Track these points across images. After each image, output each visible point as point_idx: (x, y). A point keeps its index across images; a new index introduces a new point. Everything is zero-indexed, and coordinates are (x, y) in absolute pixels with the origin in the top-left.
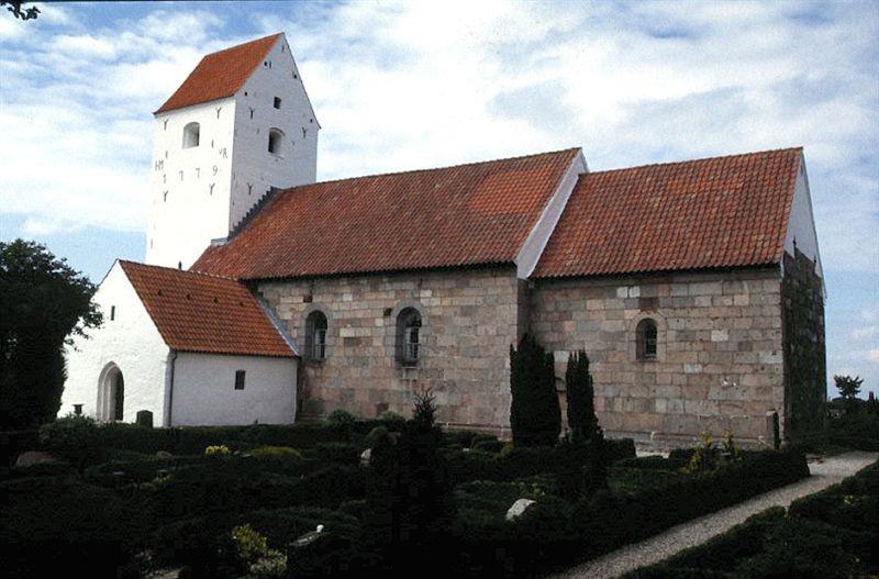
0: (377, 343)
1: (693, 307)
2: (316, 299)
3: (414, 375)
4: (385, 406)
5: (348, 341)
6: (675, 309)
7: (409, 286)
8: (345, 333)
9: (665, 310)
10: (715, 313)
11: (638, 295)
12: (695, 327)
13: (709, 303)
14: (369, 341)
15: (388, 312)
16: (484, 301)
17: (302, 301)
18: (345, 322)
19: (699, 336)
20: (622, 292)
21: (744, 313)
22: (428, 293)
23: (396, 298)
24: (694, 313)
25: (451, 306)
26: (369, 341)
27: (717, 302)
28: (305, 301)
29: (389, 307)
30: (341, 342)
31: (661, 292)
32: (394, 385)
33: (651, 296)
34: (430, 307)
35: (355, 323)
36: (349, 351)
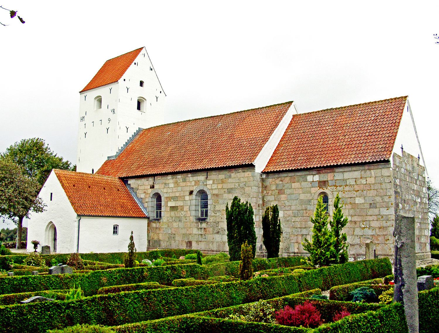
0: (186, 208)
1: (346, 185)
2: (156, 186)
3: (204, 225)
4: (190, 243)
5: (173, 208)
6: (337, 186)
7: (201, 177)
8: (171, 204)
9: (332, 187)
10: (357, 188)
11: (318, 180)
12: (347, 196)
13: (354, 183)
14: (182, 208)
15: (191, 193)
16: (239, 185)
17: (149, 187)
18: (169, 199)
20: (310, 178)
21: (372, 187)
22: (211, 182)
23: (195, 185)
24: (347, 188)
25: (222, 188)
26: (182, 208)
27: (358, 182)
28: (151, 188)
29: (192, 190)
30: (169, 208)
31: (328, 176)
32: (195, 231)
33: (325, 180)
34: (212, 189)
35: (175, 198)
36: (173, 213)
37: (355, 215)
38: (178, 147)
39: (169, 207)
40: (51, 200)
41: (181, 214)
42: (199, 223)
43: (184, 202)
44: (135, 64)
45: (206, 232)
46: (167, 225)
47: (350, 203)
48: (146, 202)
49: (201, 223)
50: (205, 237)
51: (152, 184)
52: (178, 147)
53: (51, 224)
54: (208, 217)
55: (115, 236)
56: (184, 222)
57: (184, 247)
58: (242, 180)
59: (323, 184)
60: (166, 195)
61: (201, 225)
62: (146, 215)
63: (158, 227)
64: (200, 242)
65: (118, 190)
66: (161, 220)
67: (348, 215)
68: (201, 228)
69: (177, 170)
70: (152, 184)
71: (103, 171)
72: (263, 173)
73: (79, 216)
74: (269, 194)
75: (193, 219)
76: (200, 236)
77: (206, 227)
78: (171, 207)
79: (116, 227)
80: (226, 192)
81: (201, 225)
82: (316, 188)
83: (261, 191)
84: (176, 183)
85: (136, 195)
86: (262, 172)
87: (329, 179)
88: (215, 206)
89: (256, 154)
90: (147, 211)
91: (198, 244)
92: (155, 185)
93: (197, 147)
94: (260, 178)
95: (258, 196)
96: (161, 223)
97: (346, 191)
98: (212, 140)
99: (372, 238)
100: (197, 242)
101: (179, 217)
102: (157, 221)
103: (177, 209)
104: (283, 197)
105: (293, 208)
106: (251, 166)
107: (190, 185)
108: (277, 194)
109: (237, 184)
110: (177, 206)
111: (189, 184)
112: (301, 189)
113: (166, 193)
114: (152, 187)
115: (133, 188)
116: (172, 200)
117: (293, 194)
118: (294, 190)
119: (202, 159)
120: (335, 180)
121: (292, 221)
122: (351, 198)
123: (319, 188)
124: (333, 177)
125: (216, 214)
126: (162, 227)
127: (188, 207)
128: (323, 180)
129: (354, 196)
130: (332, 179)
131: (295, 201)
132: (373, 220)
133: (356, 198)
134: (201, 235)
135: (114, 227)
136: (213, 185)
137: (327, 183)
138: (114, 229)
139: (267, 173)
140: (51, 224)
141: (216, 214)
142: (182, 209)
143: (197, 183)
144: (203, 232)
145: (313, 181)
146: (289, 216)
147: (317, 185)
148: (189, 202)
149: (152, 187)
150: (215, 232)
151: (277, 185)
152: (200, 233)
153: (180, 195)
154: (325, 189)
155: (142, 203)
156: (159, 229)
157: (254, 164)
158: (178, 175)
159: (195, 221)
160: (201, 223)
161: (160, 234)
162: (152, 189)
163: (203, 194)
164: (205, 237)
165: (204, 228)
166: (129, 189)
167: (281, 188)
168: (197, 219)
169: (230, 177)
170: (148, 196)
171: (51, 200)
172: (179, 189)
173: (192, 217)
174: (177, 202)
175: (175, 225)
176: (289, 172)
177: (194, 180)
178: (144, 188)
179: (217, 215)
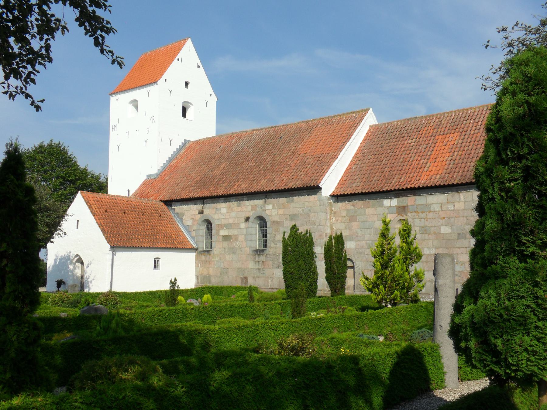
0: (242, 238)
1: (430, 211)
2: (206, 212)
3: (262, 258)
4: (246, 279)
5: (226, 238)
6: (419, 213)
7: (259, 202)
8: (223, 233)
9: (413, 214)
11: (396, 204)
12: (430, 225)
13: (439, 209)
14: (236, 238)
15: (247, 219)
16: (303, 210)
17: (198, 212)
18: (221, 226)
19: (433, 229)
20: (387, 202)
22: (270, 207)
23: (252, 210)
24: (431, 215)
25: (284, 215)
26: (236, 238)
27: (444, 208)
28: (199, 213)
29: (248, 216)
30: (221, 238)
31: (409, 200)
32: (251, 265)
33: (405, 204)
34: (271, 215)
35: (228, 226)
36: (225, 244)
37: (441, 247)
38: (232, 164)
39: (221, 237)
40: (77, 228)
41: (235, 244)
42: (257, 256)
43: (239, 230)
44: (178, 60)
45: (265, 266)
46: (219, 258)
47: (435, 233)
48: (194, 230)
49: (259, 255)
50: (263, 272)
51: (201, 209)
52: (232, 164)
53: (78, 257)
54: (268, 249)
55: (156, 271)
56: (238, 254)
57: (239, 284)
58: (306, 204)
59: (402, 209)
60: (217, 223)
61: (259, 257)
62: (194, 246)
63: (208, 260)
64: (257, 279)
65: (160, 216)
66: (212, 252)
67: (432, 247)
68: (259, 262)
69: (231, 192)
70: (201, 209)
71: (141, 193)
72: (332, 196)
73: (112, 247)
74: (339, 221)
75: (248, 250)
76: (257, 271)
77: (264, 260)
78: (223, 236)
79: (158, 261)
80: (288, 219)
81: (259, 257)
82: (394, 214)
83: (329, 217)
84: (229, 208)
85: (182, 221)
86: (330, 195)
87: (409, 204)
88: (275, 235)
89: (322, 174)
90: (194, 241)
91: (256, 281)
92: (204, 210)
93: (254, 164)
94: (328, 202)
95: (325, 223)
96: (212, 255)
97: (430, 219)
98: (273, 156)
99: (461, 274)
100: (254, 277)
101: (233, 248)
102: (206, 253)
103: (230, 239)
104: (355, 225)
105: (367, 237)
106: (315, 189)
107: (246, 210)
108: (348, 221)
109: (301, 210)
110: (231, 236)
111: (244, 209)
112: (376, 216)
113: (218, 219)
114: (201, 212)
115: (178, 213)
116: (225, 228)
117: (367, 221)
118: (368, 216)
119: (261, 179)
120: (417, 205)
121: (366, 253)
122: (435, 226)
123: (397, 215)
124: (415, 201)
125: (276, 244)
126: (213, 260)
127: (243, 236)
128: (402, 205)
129: (440, 224)
130: (413, 204)
131: (369, 230)
132: (462, 253)
133: (442, 227)
134: (259, 269)
135: (155, 261)
136: (273, 210)
137: (406, 208)
138: (155, 262)
139: (337, 197)
140: (78, 257)
141: (276, 244)
142: (236, 239)
143: (254, 208)
144: (261, 266)
145: (391, 206)
146: (362, 247)
147: (395, 210)
148: (245, 230)
149: (201, 212)
150: (275, 266)
151: (348, 210)
152: (257, 267)
153: (234, 221)
154: (405, 216)
155: (189, 232)
156: (209, 262)
157: (321, 187)
158: (232, 198)
159: (251, 253)
160: (259, 255)
161: (211, 269)
162: (201, 215)
163: (262, 221)
164: (263, 272)
165: (262, 262)
166: (173, 215)
167: (353, 215)
168: (254, 251)
169: (293, 201)
170: (196, 222)
171: (77, 228)
172: (233, 214)
173: (248, 248)
174: (231, 230)
175: (228, 257)
176: (311, 189)
177: (251, 204)
178: (191, 214)
179: (278, 246)
